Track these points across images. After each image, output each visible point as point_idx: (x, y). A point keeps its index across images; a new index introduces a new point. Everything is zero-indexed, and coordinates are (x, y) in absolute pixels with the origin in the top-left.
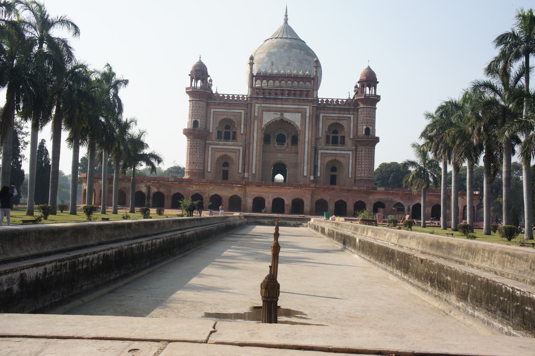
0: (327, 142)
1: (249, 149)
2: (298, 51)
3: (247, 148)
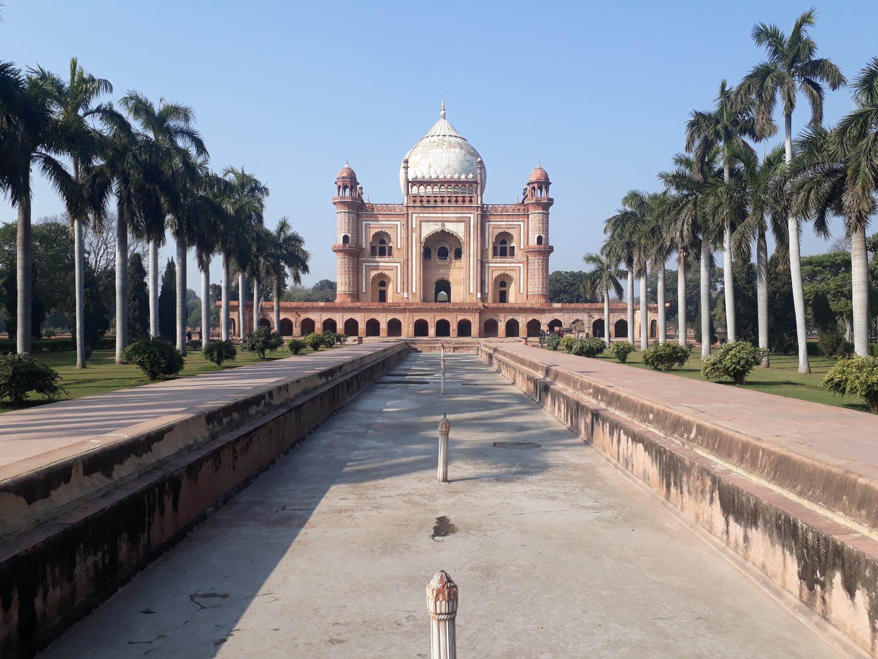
0: (495, 255)
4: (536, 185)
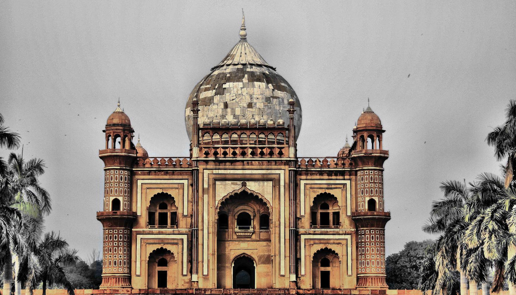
0: (313, 223)
1: (197, 238)
2: (263, 85)
4: (365, 134)
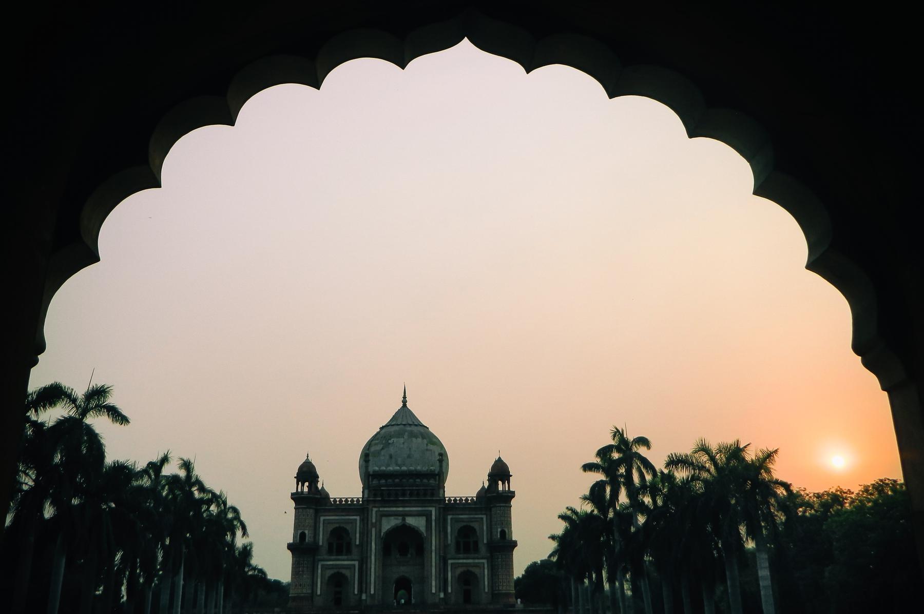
0: (458, 550)
2: (420, 440)
3: (364, 561)
